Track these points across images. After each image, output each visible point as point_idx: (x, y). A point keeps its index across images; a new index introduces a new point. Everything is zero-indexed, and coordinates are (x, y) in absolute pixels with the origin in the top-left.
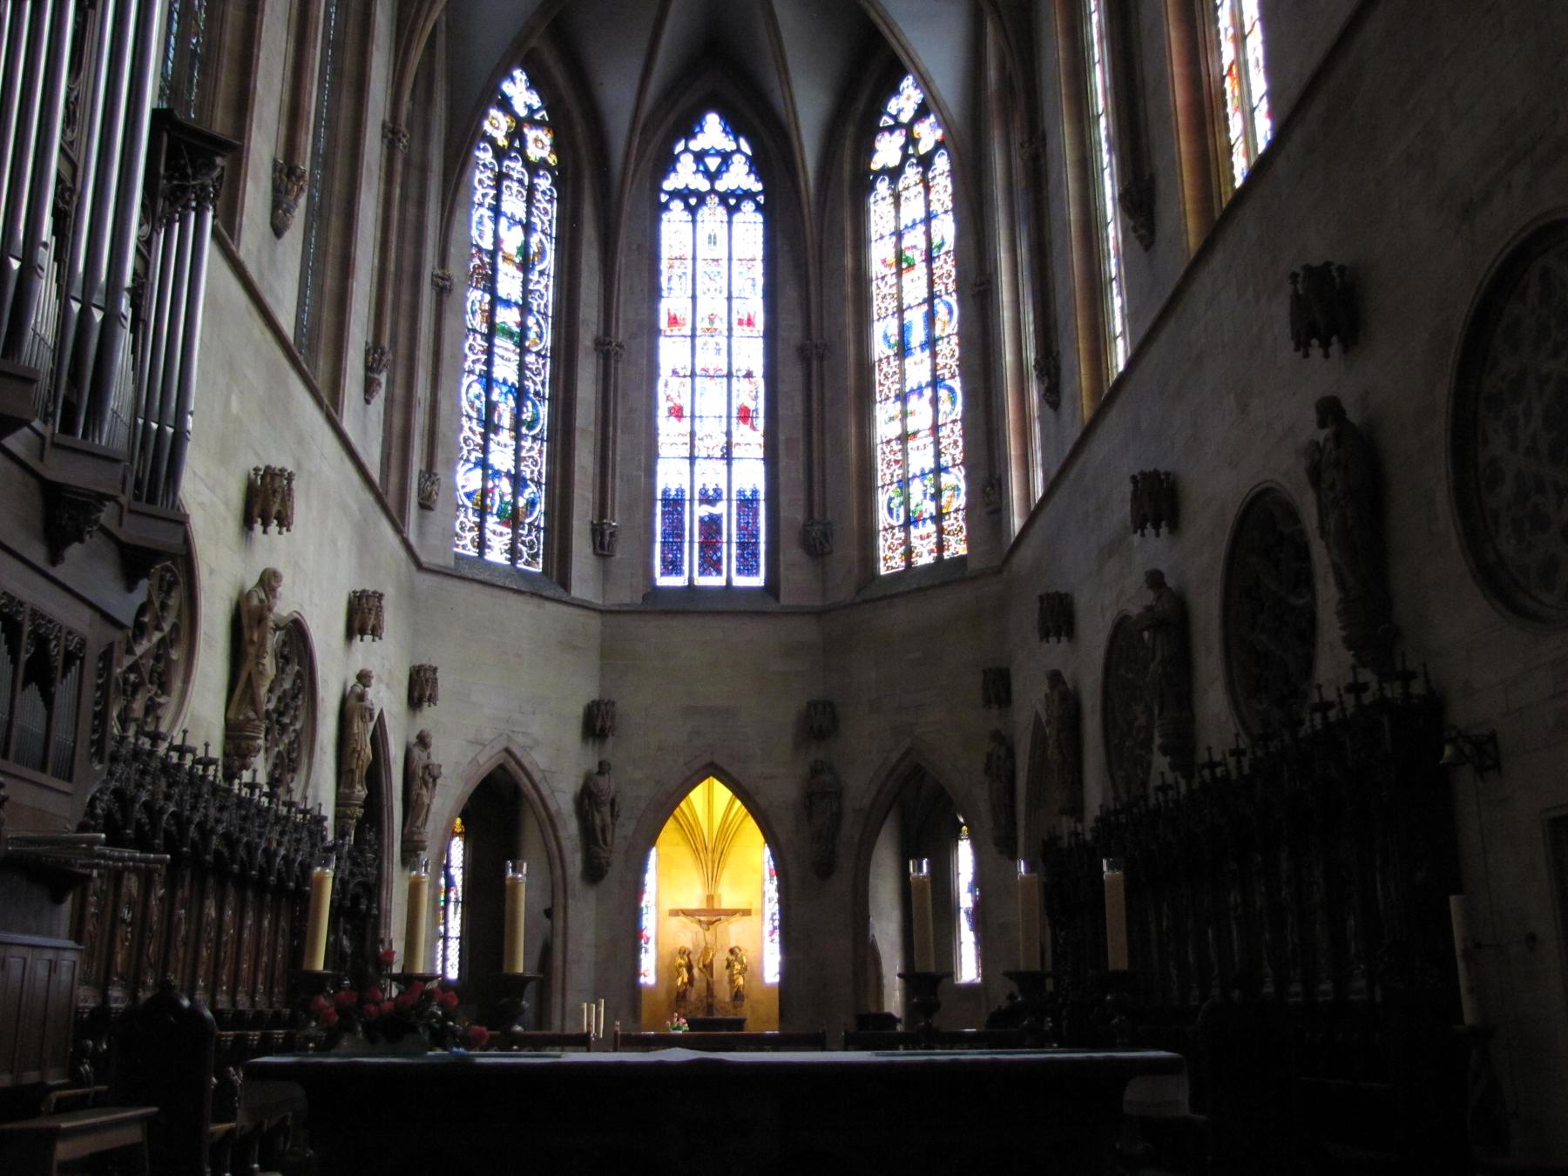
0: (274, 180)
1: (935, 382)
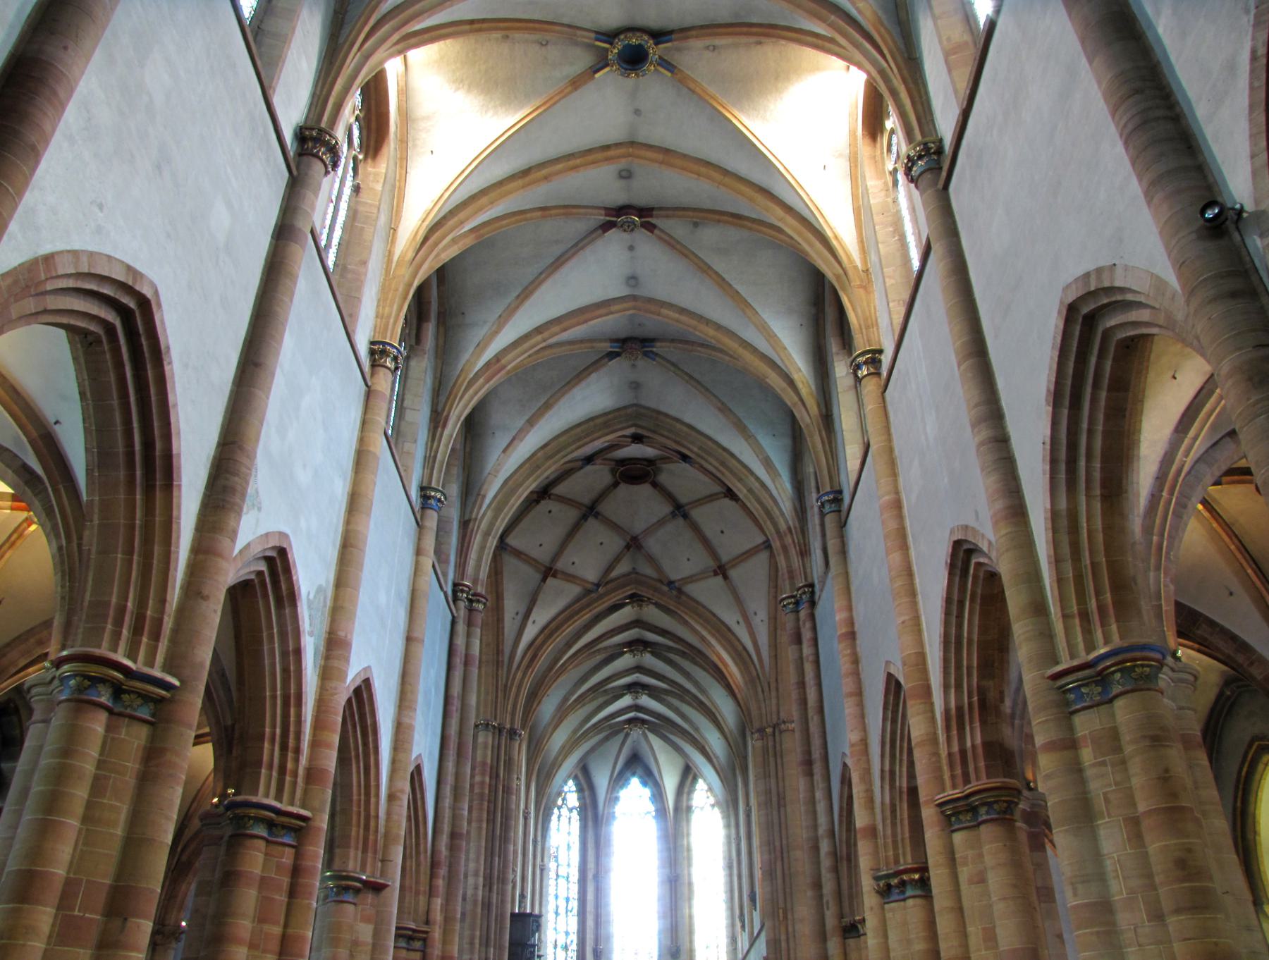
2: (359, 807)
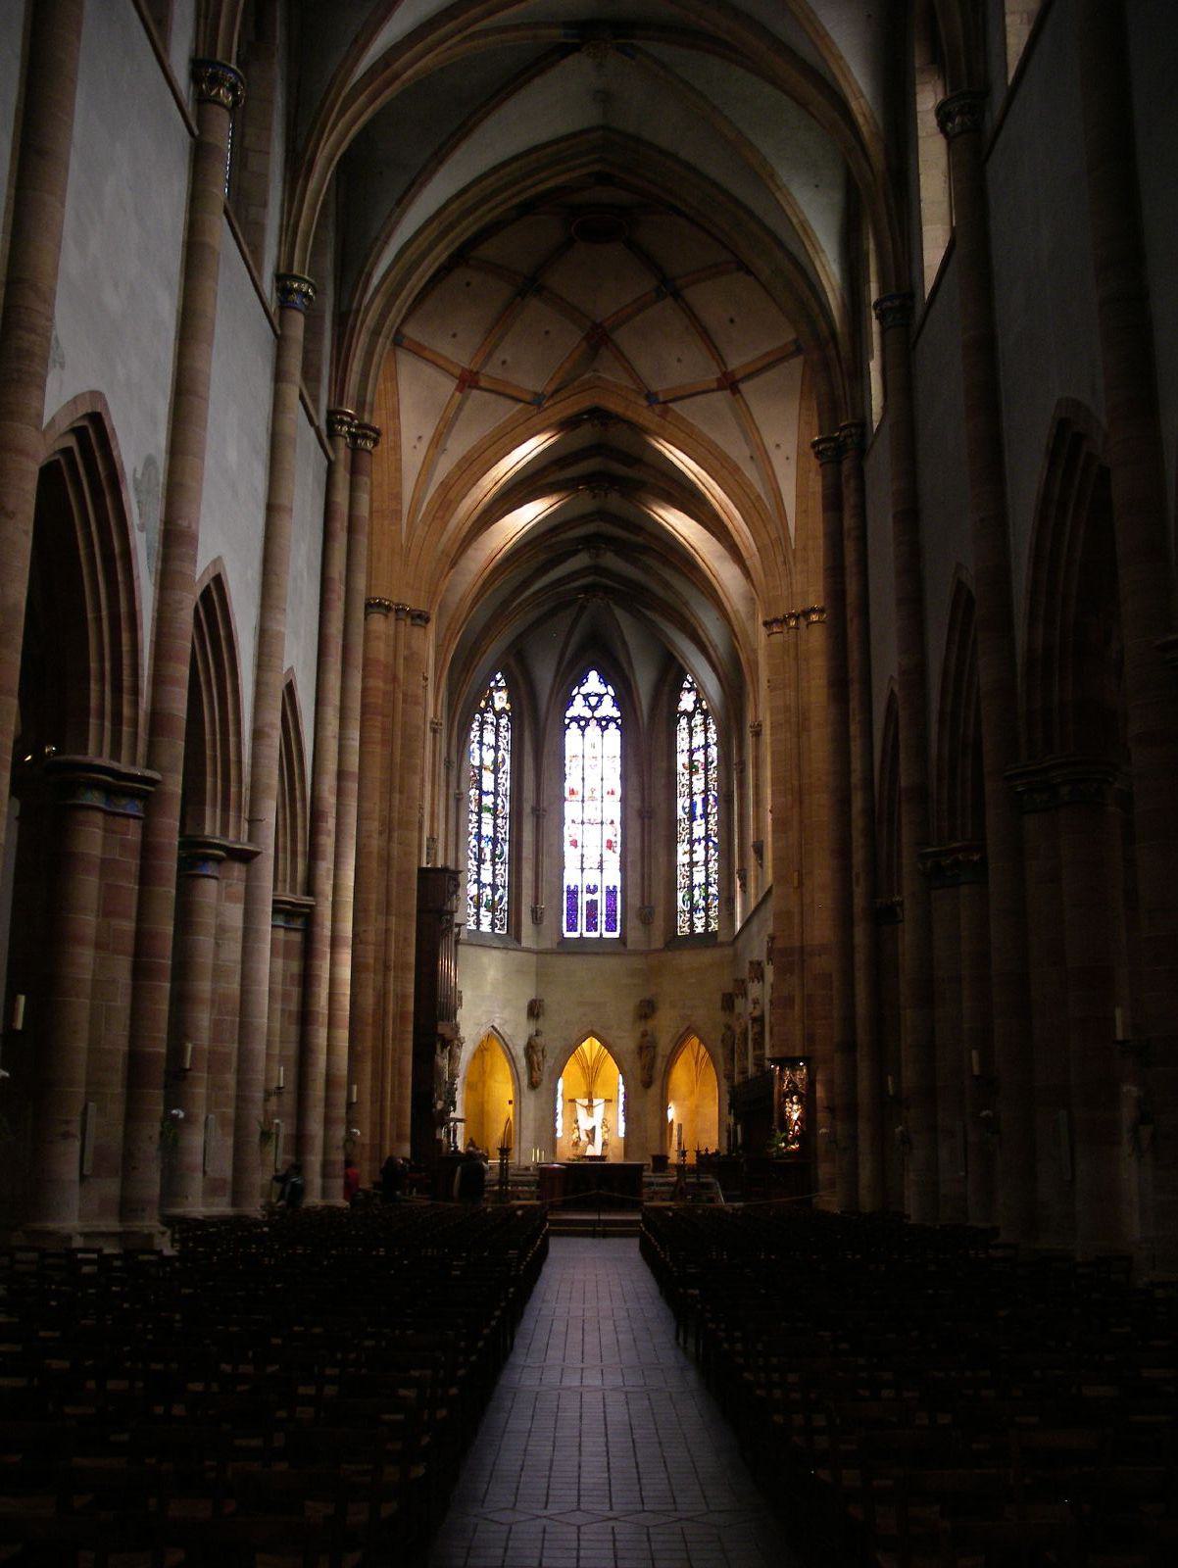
1: (707, 838)
2: (215, 751)
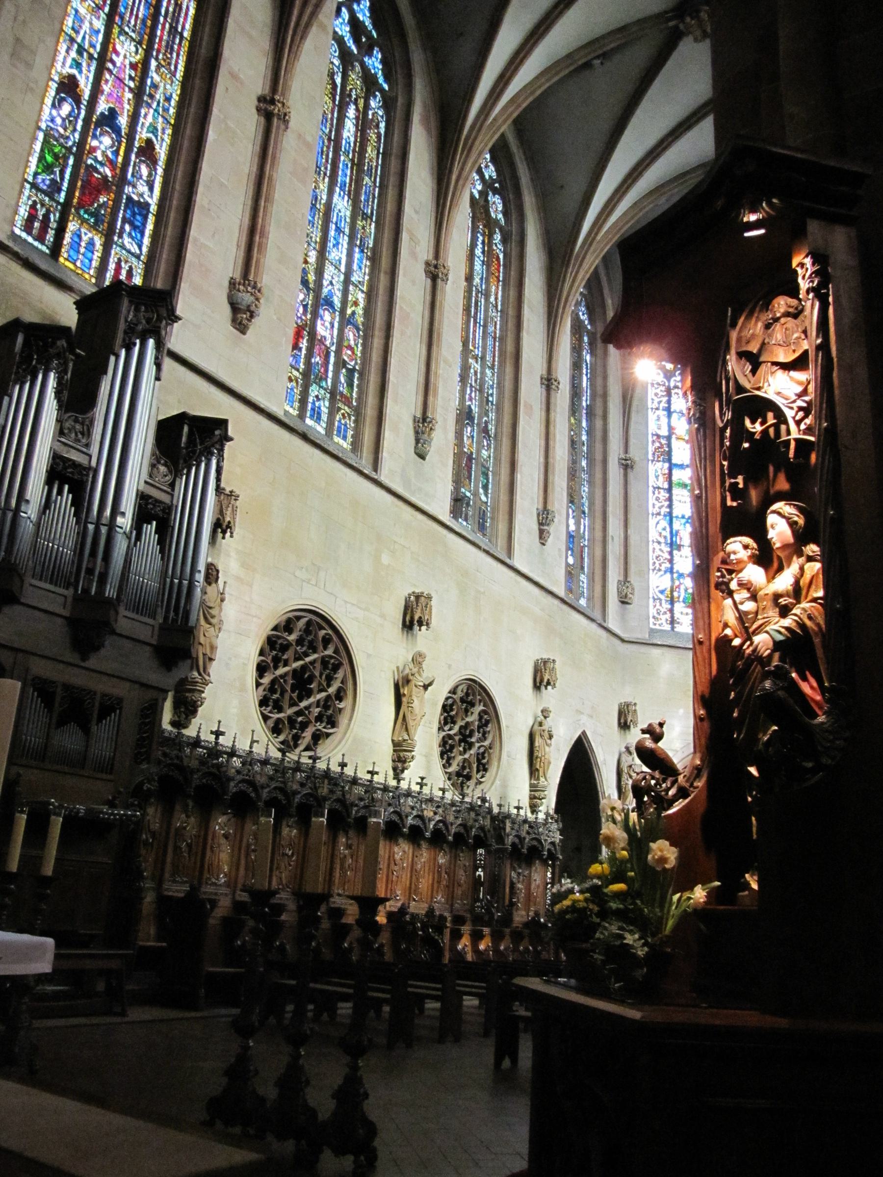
0: (415, 428)
